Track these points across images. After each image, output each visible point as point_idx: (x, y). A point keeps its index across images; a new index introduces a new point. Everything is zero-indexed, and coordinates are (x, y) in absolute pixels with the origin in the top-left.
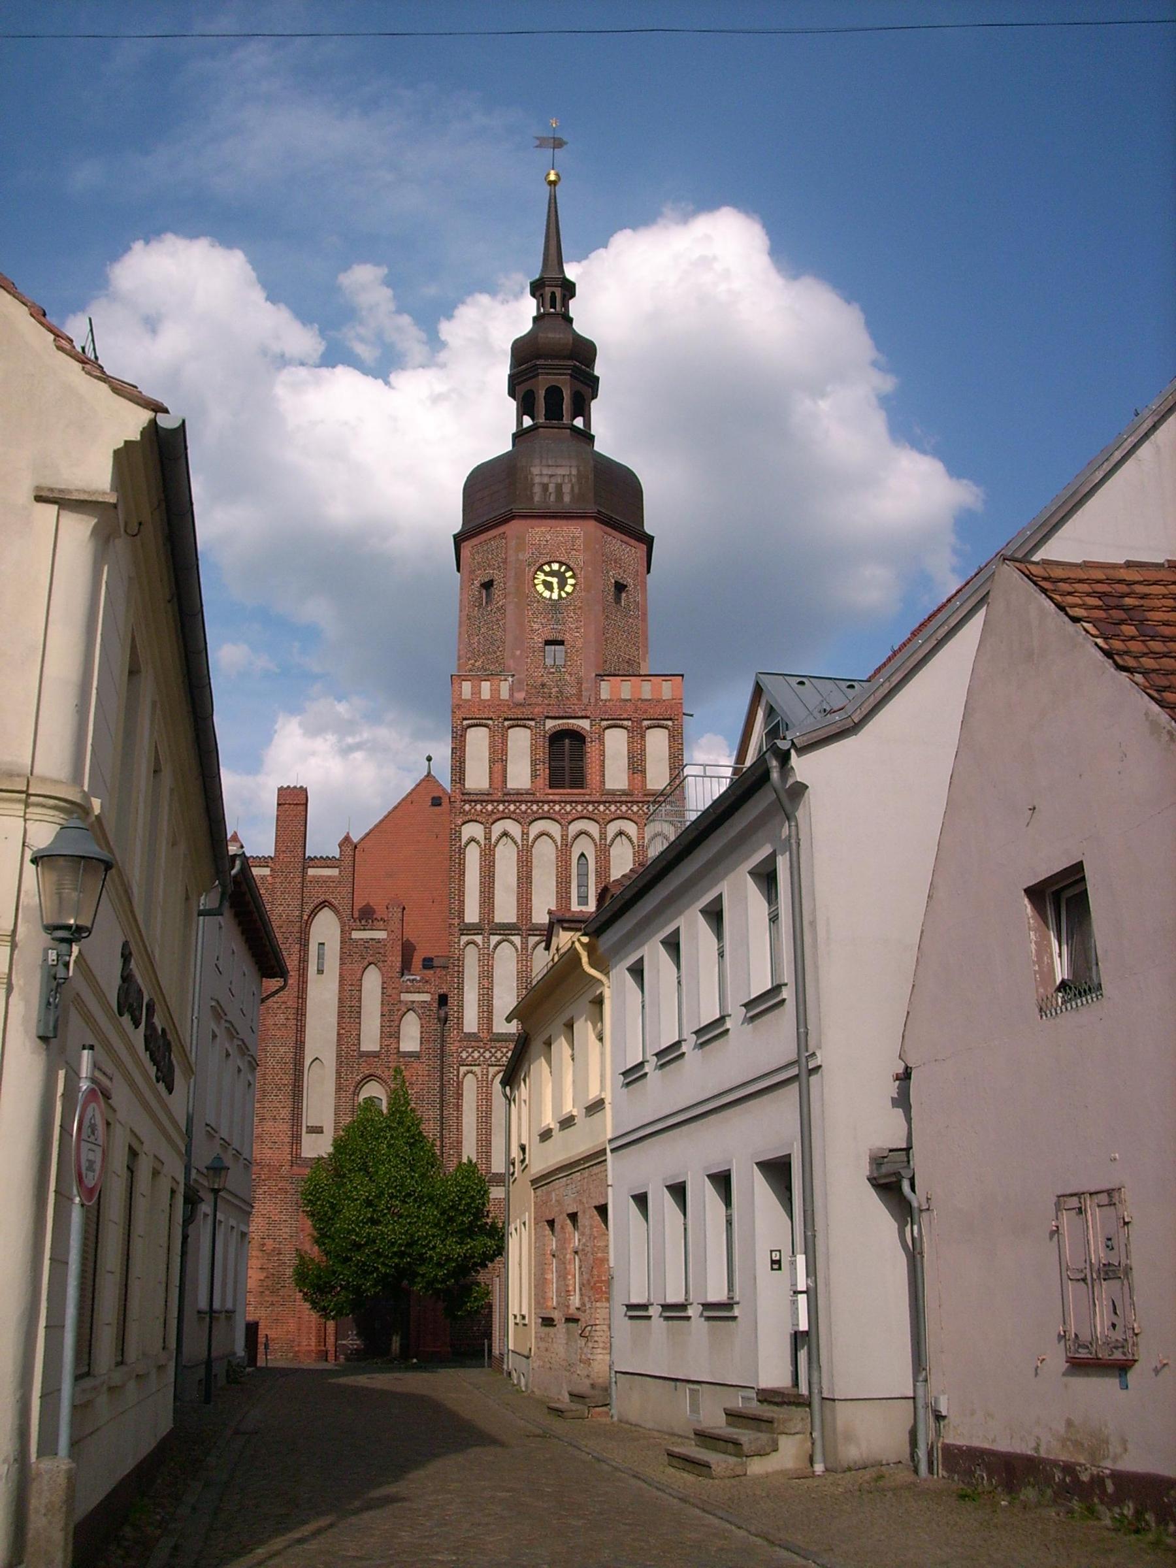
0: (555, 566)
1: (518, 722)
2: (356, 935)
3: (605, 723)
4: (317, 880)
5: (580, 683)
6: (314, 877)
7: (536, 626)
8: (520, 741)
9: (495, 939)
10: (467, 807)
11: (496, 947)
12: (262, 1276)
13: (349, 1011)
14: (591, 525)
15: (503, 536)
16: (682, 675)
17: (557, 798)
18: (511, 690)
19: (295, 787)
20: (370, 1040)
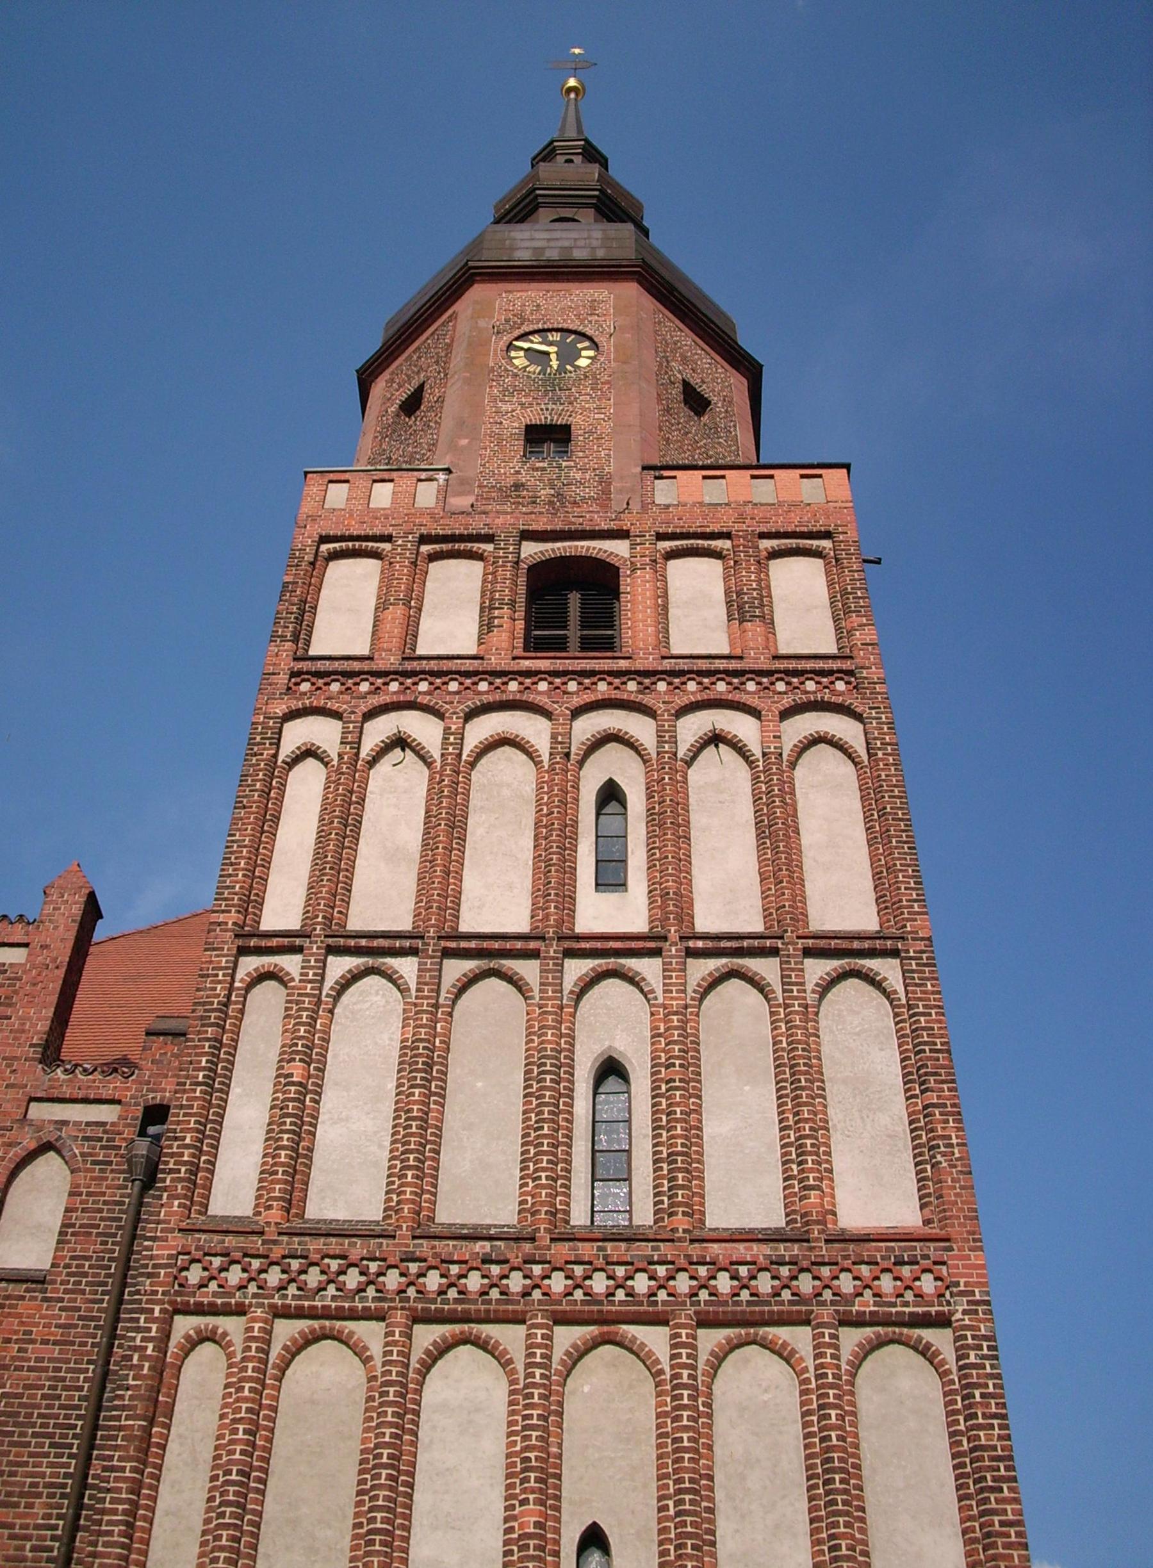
1: (453, 545)
5: (605, 482)
14: (631, 290)
16: (847, 467)
17: (543, 665)
18: (444, 493)
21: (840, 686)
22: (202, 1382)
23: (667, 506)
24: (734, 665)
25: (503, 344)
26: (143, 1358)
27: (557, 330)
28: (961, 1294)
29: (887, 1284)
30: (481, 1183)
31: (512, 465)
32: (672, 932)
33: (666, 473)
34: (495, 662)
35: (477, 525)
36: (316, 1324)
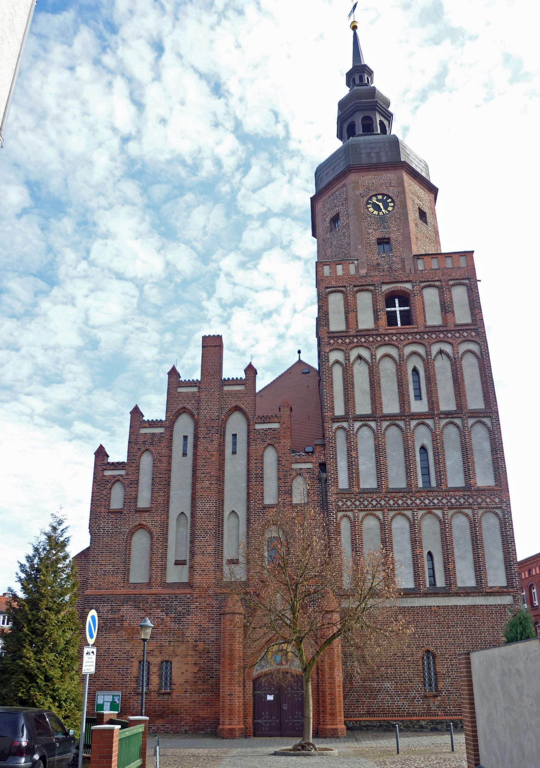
0: (380, 197)
1: (362, 288)
2: (258, 427)
3: (423, 284)
4: (230, 393)
6: (228, 391)
7: (370, 231)
8: (364, 300)
9: (357, 425)
10: (332, 341)
11: (359, 429)
12: (196, 669)
13: (254, 477)
15: (344, 185)
18: (357, 268)
19: (214, 336)
20: (270, 496)
21: (473, 334)
22: (345, 525)
23: (422, 271)
24: (445, 329)
25: (365, 202)
26: (334, 522)
27: (380, 194)
28: (504, 502)
29: (488, 500)
30: (397, 479)
31: (375, 255)
32: (433, 412)
33: (420, 257)
34: (381, 331)
35: (369, 280)
36: (368, 512)
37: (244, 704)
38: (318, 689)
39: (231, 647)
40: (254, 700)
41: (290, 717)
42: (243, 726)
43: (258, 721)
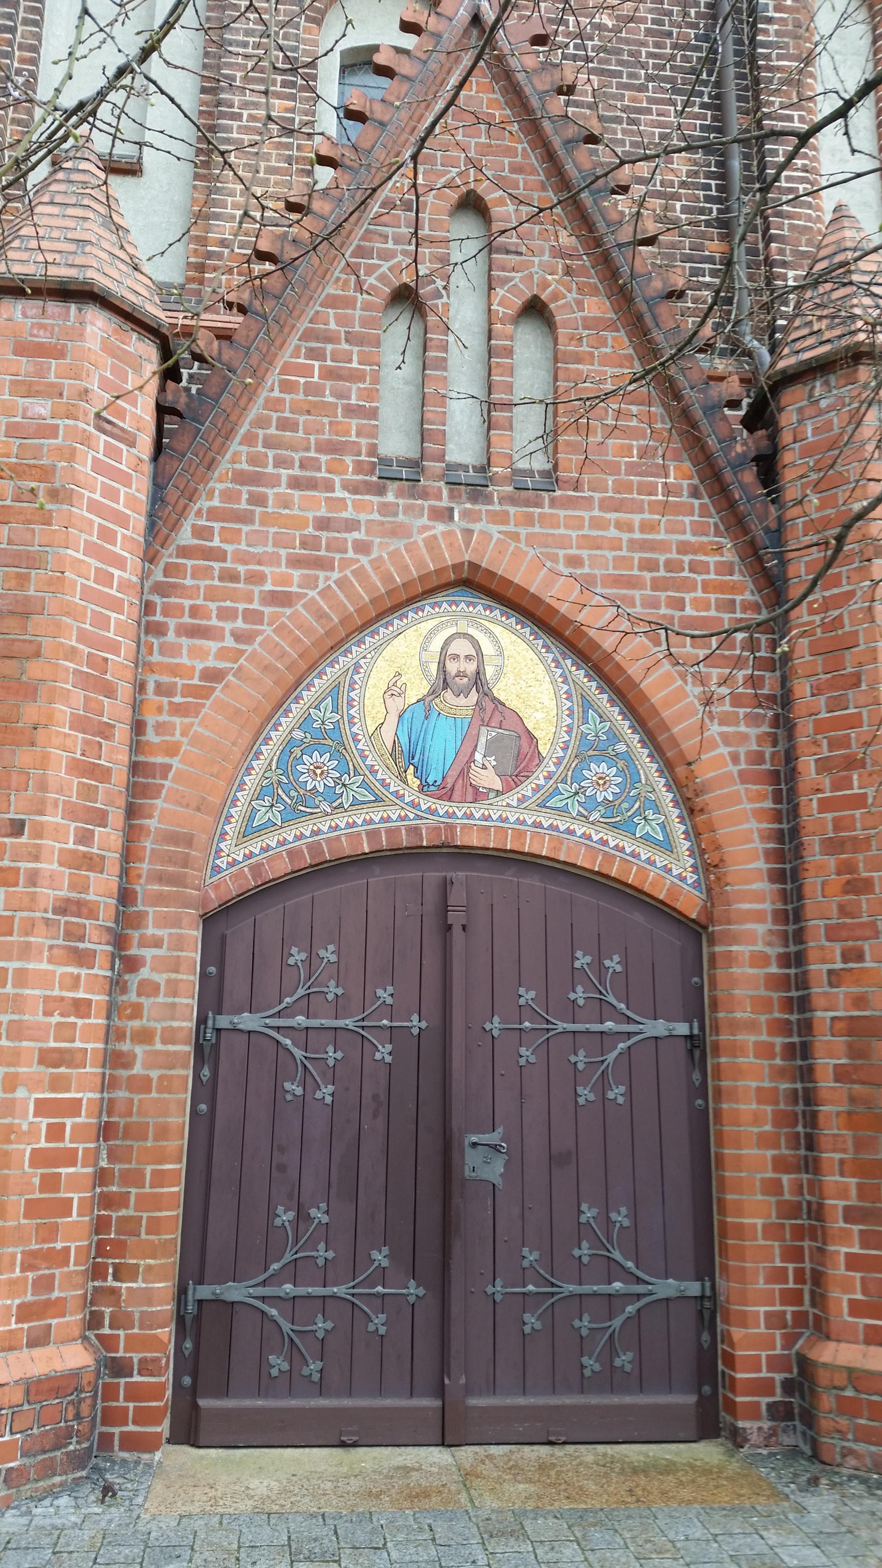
37: (106, 1131)
38: (804, 1004)
39: (23, 580)
40: (205, 1092)
41: (531, 1256)
42: (75, 1357)
43: (234, 1292)
